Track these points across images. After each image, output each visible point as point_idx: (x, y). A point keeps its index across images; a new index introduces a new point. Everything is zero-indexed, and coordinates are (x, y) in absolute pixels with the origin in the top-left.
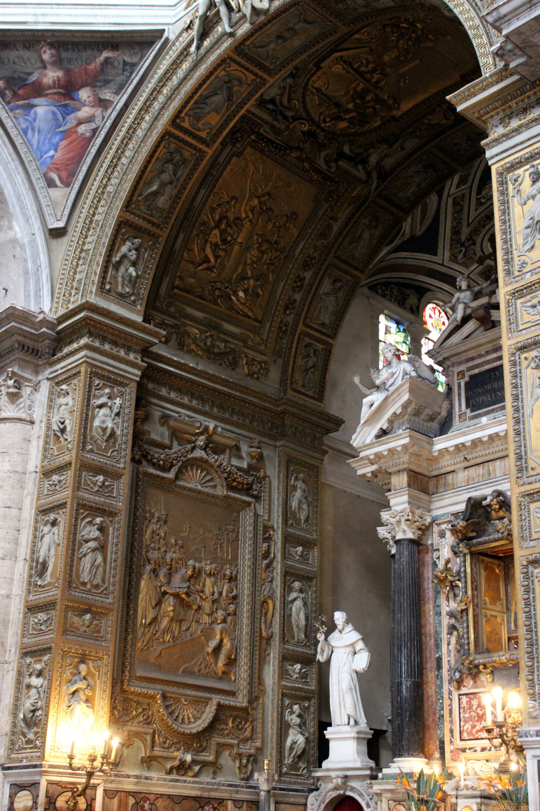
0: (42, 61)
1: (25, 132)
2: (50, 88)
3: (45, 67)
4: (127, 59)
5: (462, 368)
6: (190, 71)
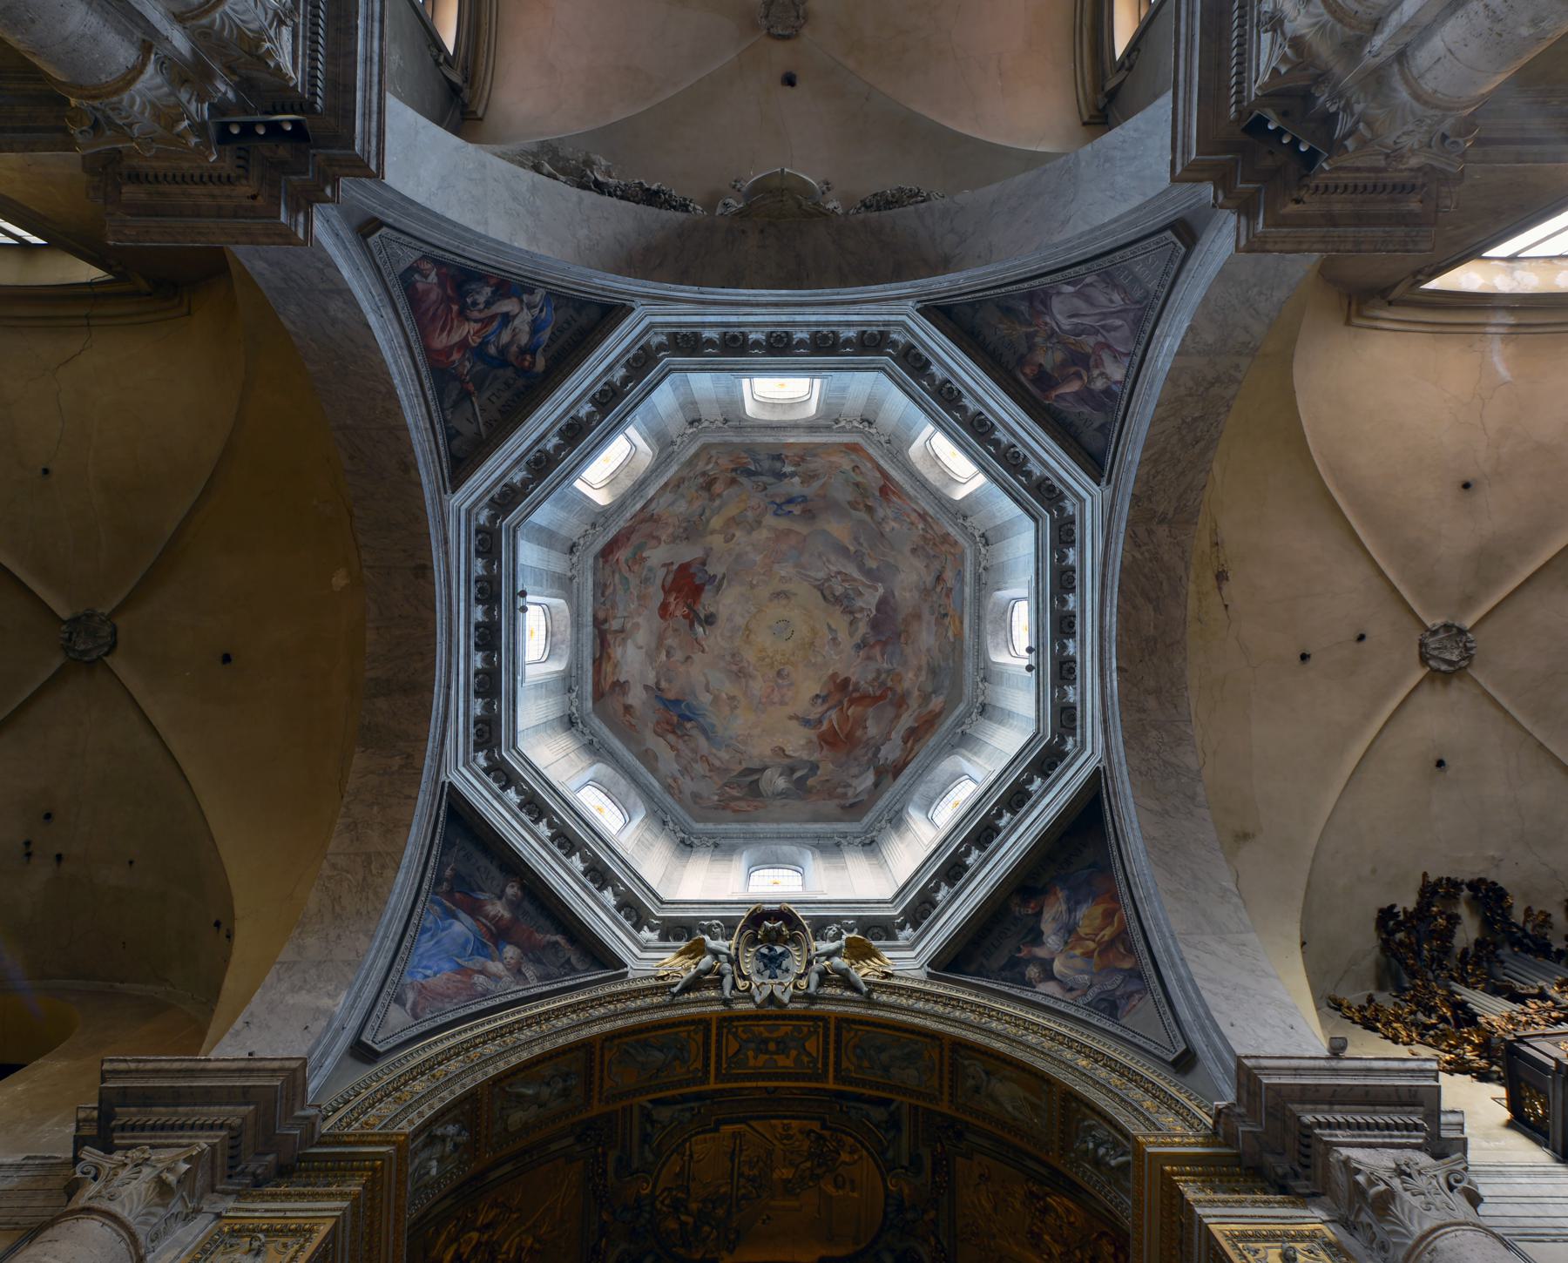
0: (503, 891)
2: (486, 917)
3: (500, 898)
4: (574, 960)
6: (656, 1007)
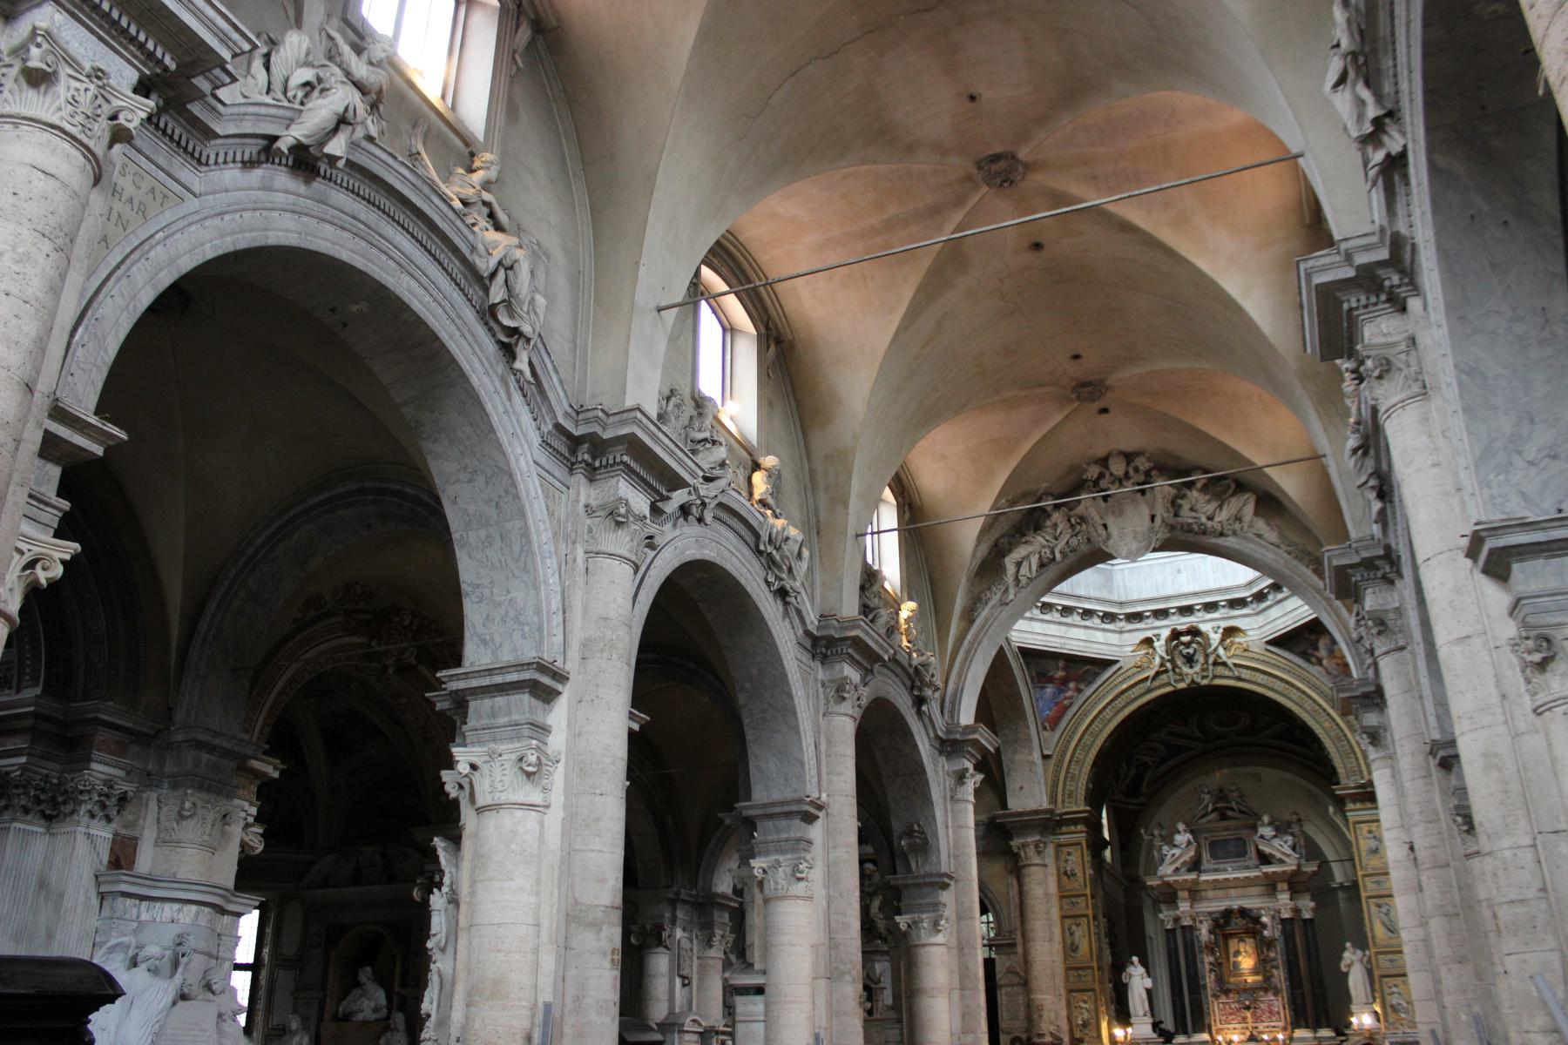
1: (1037, 700)
3: (1058, 670)
4: (1097, 670)
5: (1207, 835)
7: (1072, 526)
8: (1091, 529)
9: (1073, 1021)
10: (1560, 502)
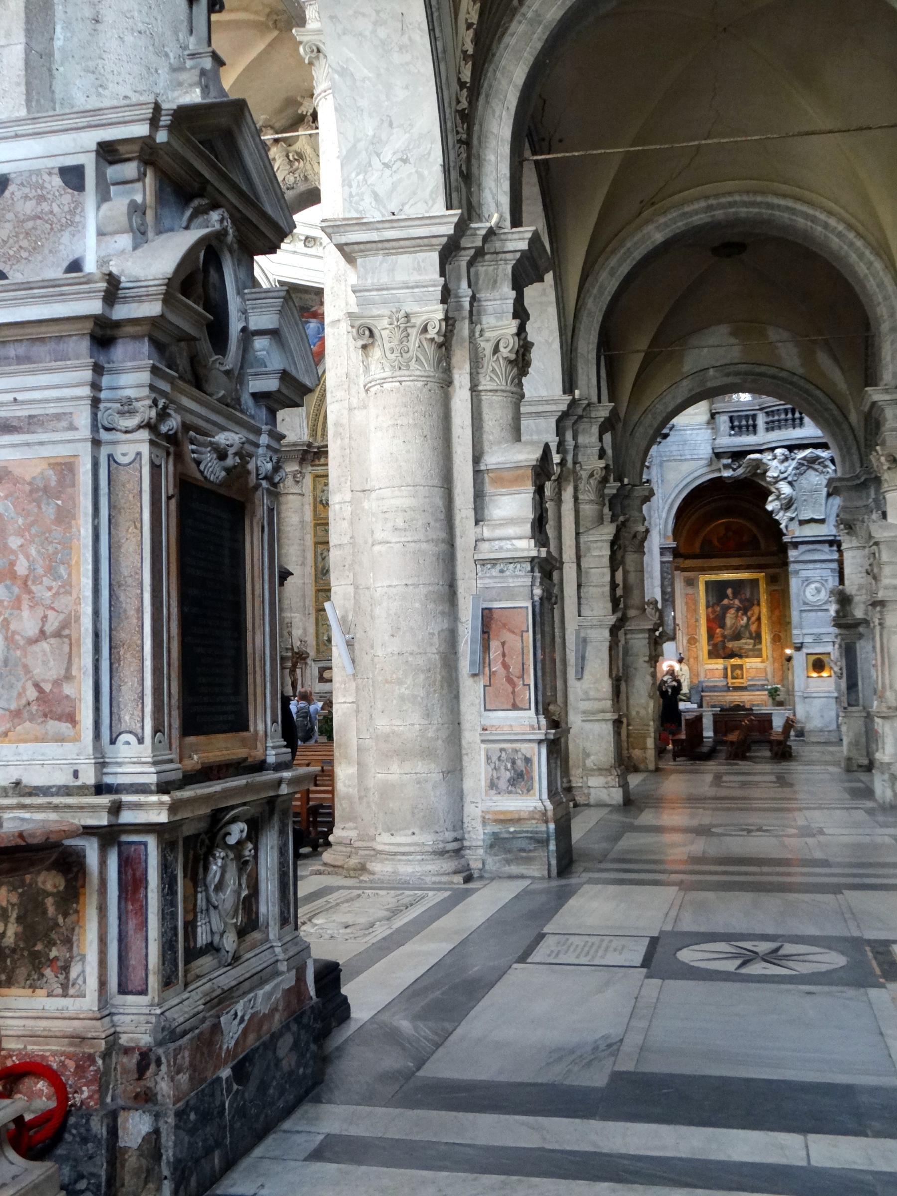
7: (290, 163)
8: (309, 167)
9: (320, 638)
10: (403, 205)
